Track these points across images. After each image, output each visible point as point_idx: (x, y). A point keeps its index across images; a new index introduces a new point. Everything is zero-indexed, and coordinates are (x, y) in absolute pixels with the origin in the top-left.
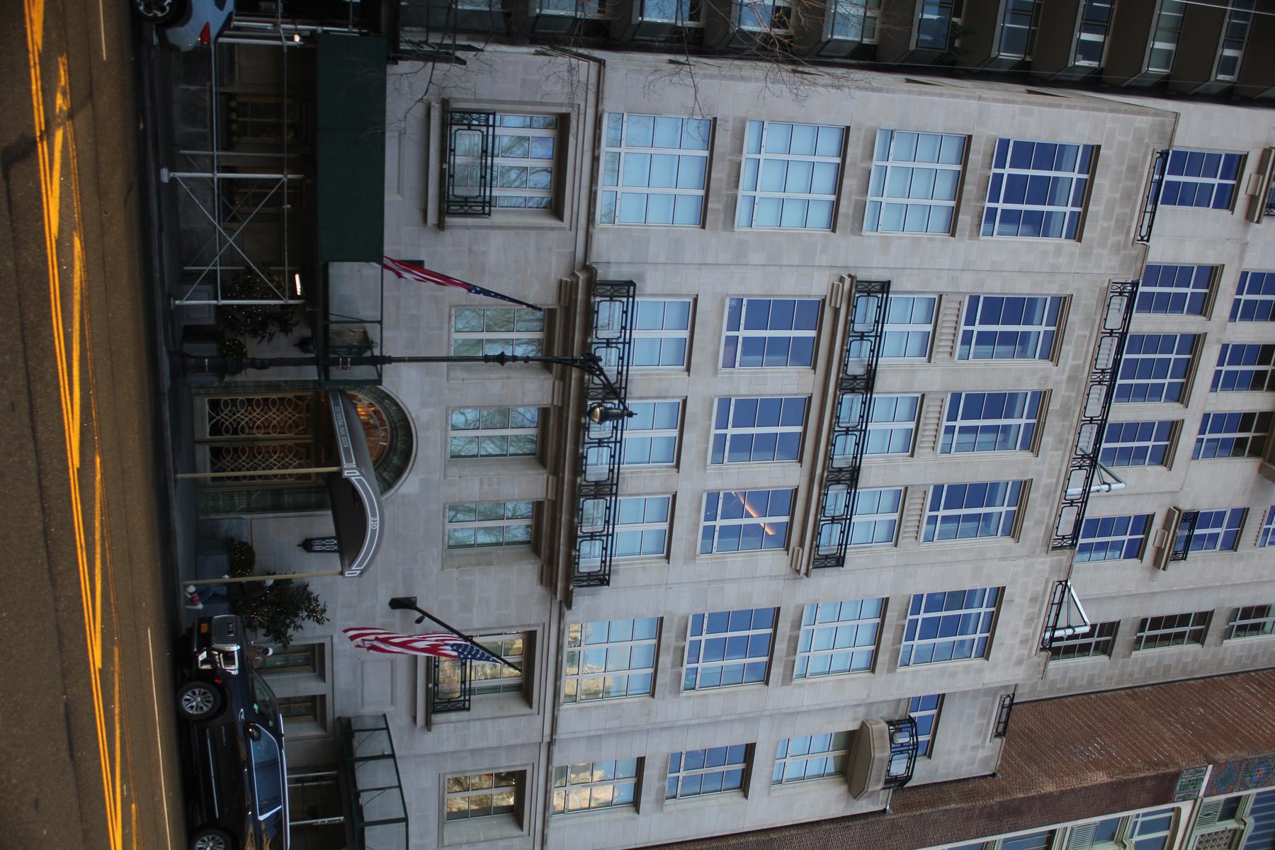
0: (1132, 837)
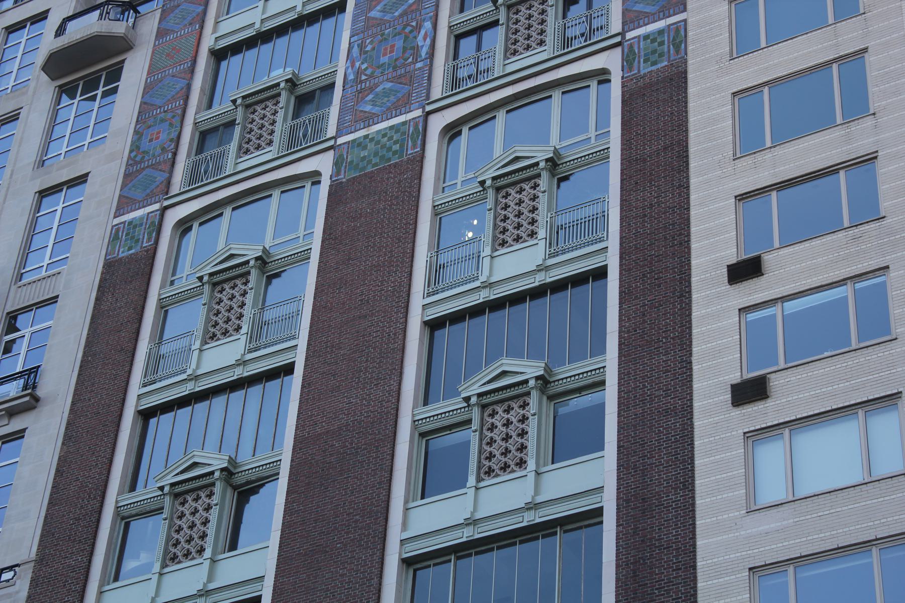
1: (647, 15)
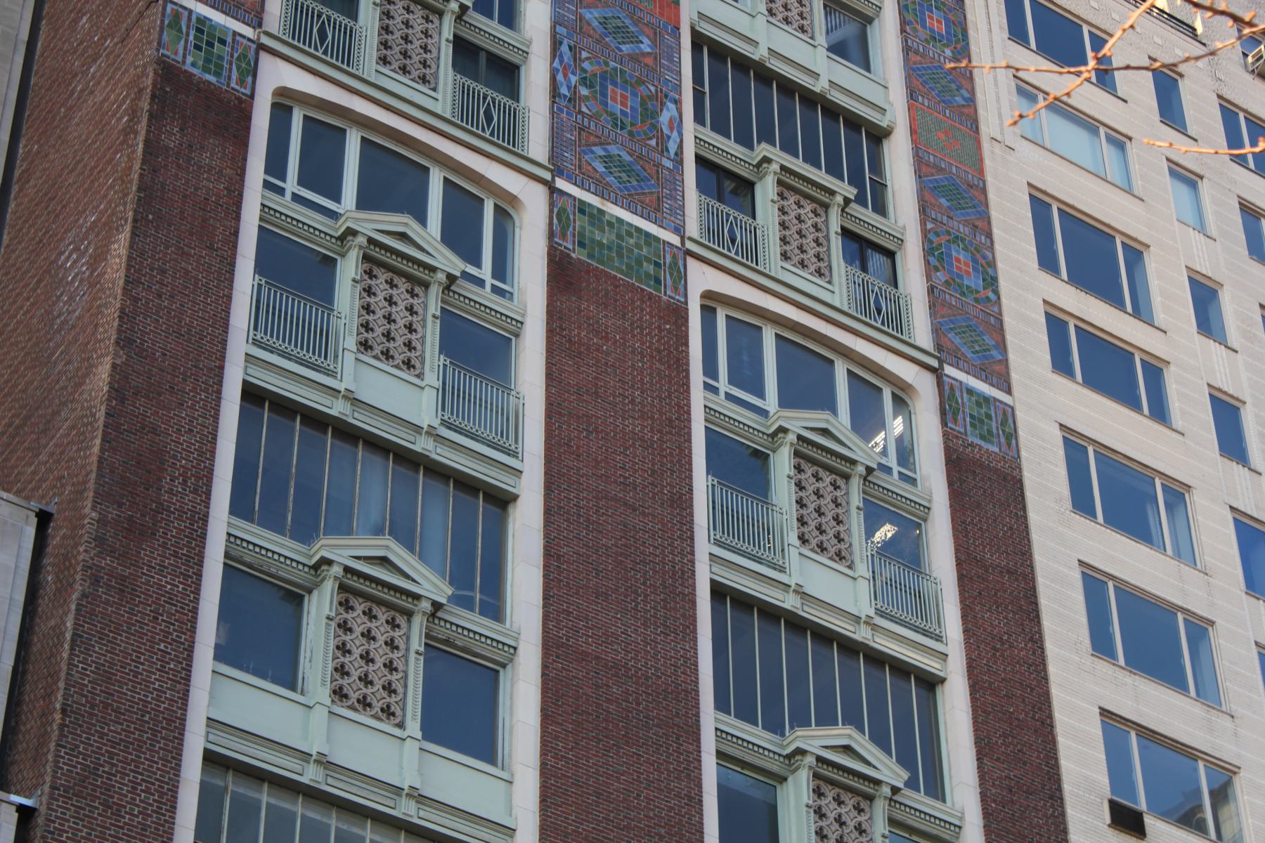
0: (764, 413)
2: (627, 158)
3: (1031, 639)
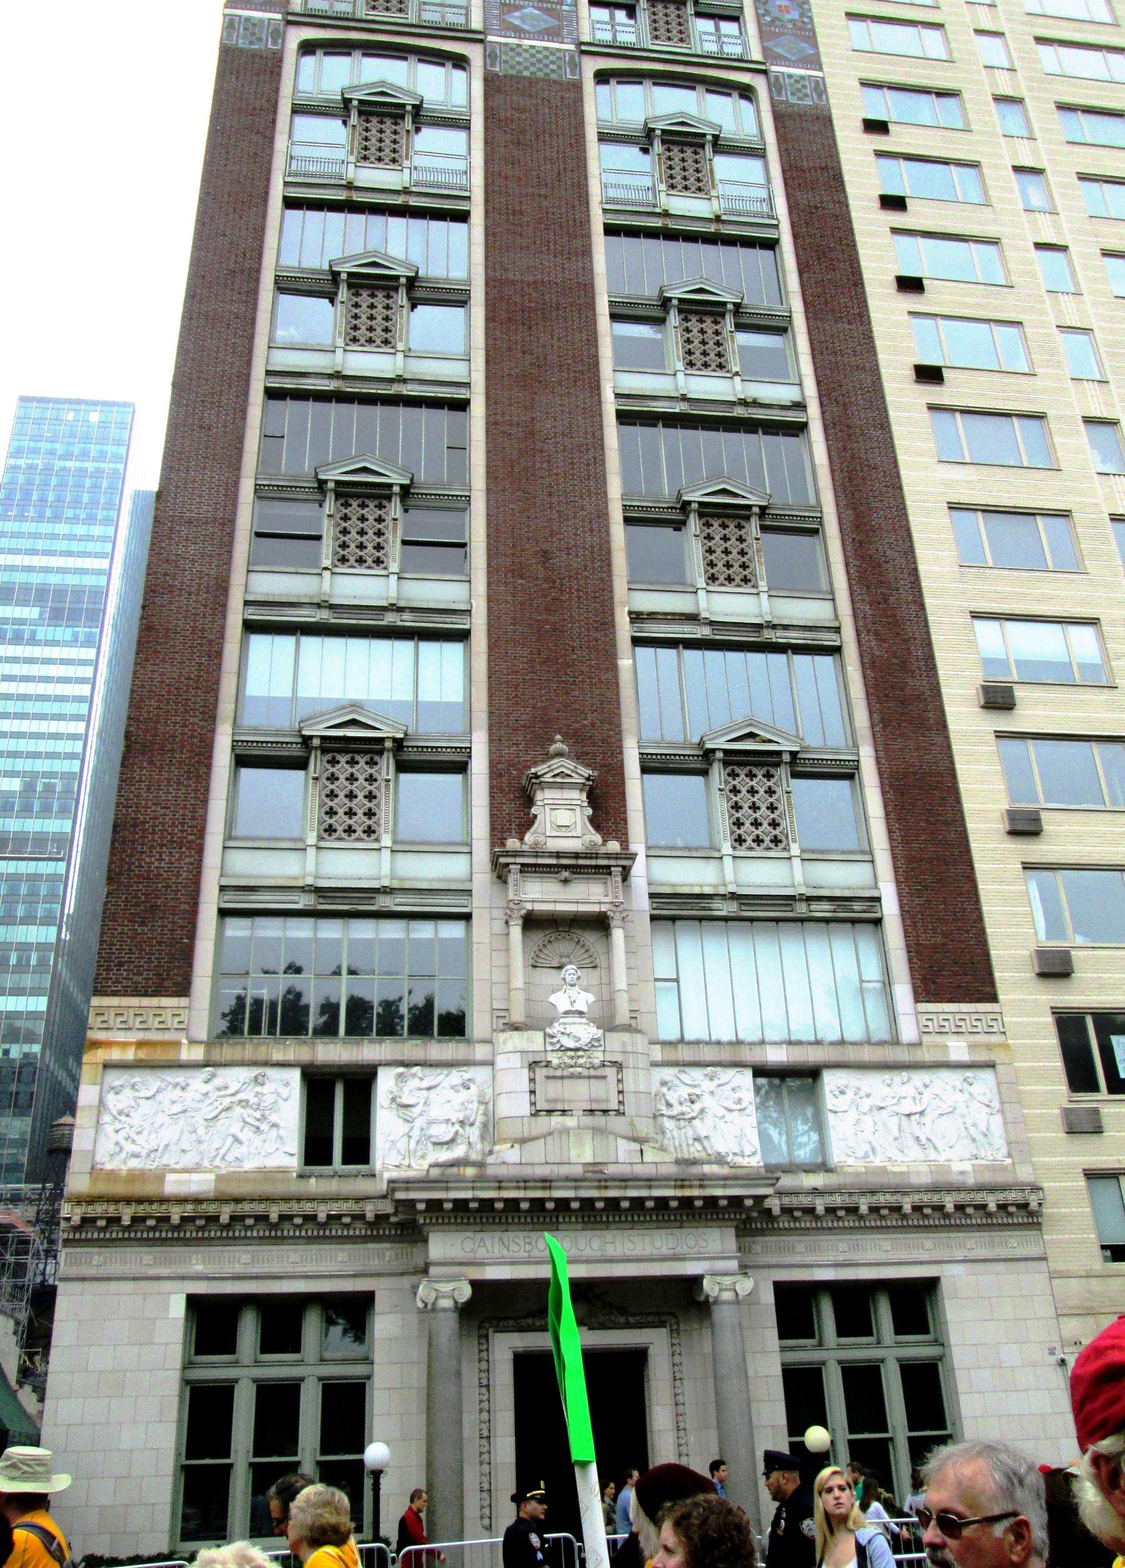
1: (786, 59)
2: (537, 12)
3: (839, 202)
